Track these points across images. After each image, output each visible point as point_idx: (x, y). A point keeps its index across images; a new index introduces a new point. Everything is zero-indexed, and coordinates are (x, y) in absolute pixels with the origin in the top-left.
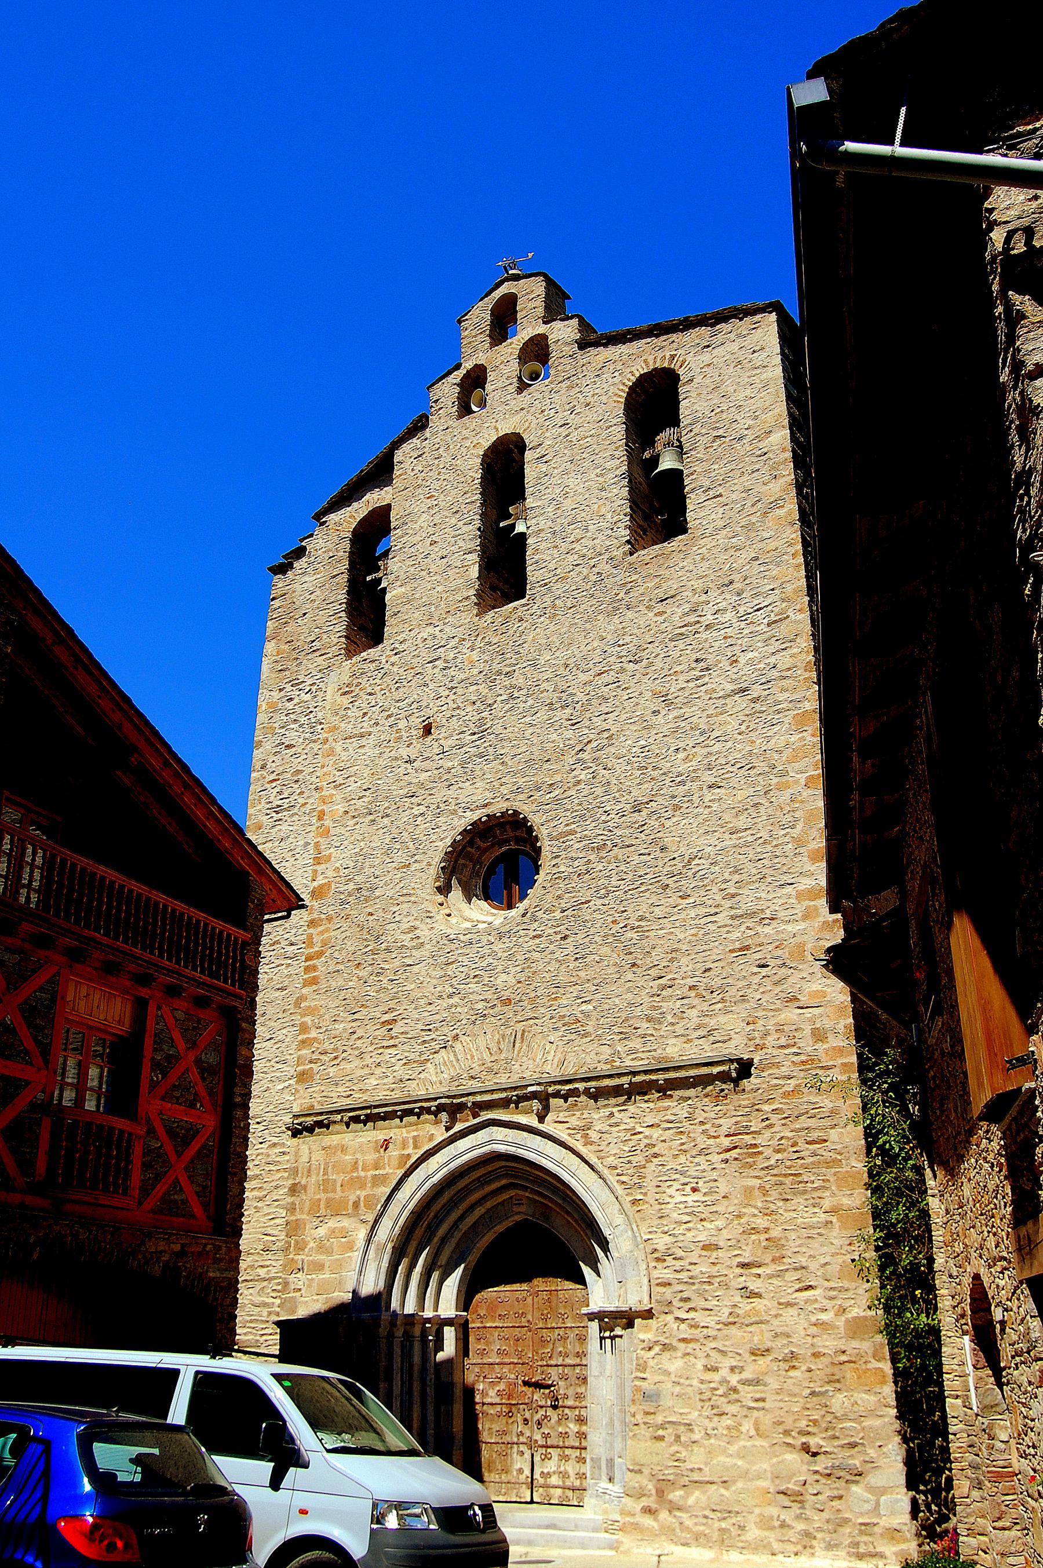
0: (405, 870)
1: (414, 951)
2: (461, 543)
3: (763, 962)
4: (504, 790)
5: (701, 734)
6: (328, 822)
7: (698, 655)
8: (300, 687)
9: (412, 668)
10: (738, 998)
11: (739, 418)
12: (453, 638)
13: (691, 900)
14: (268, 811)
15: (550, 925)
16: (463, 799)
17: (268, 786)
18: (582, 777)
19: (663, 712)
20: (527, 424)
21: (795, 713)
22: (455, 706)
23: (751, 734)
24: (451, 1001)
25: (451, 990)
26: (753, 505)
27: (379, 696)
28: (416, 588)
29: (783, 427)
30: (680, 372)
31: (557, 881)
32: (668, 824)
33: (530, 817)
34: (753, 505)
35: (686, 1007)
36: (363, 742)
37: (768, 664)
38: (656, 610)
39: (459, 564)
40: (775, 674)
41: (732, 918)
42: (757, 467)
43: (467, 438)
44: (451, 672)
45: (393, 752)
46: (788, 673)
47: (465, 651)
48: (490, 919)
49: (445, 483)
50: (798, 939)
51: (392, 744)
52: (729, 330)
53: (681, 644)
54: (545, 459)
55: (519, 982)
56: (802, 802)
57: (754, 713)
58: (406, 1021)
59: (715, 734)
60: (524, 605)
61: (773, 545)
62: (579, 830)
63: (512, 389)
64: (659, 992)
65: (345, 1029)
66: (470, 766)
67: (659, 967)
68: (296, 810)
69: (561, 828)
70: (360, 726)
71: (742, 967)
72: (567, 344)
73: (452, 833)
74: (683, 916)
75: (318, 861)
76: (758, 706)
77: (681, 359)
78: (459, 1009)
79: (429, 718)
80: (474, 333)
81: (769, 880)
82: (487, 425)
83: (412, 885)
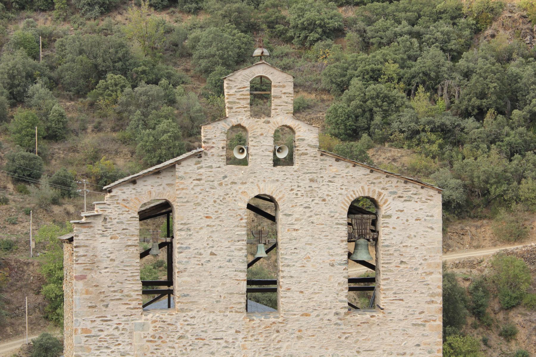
8: (109, 323)
20: (280, 196)
29: (440, 273)
43: (235, 183)
52: (415, 192)
61: (428, 340)
77: (385, 198)
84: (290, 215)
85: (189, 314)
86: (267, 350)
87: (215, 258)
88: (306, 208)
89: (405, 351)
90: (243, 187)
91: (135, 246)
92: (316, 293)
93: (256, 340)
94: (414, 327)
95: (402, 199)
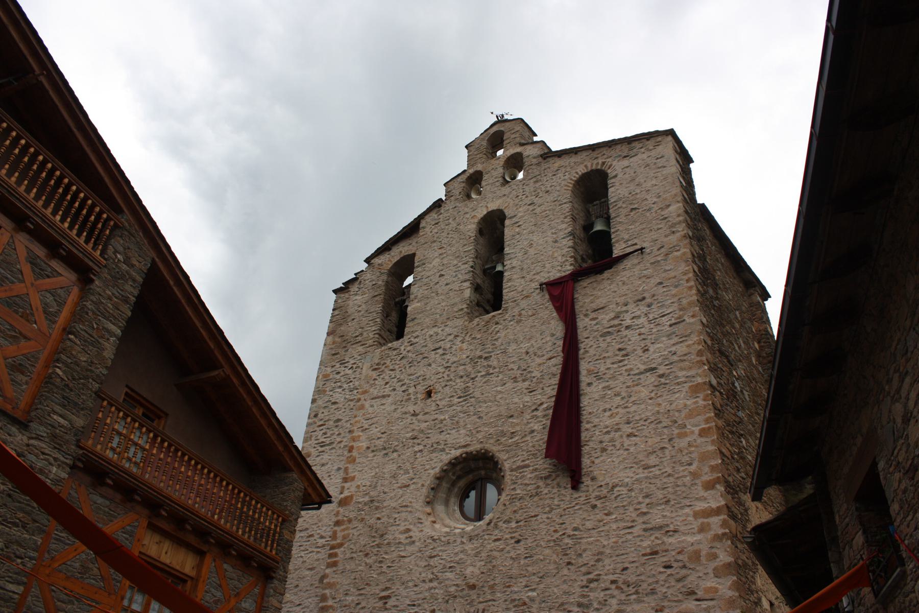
0: (405, 489)
1: (407, 548)
2: (460, 276)
3: (669, 563)
4: (480, 436)
5: (623, 398)
6: (355, 453)
7: (620, 346)
8: (346, 365)
9: (421, 354)
10: (648, 590)
11: (647, 197)
12: (450, 335)
13: (614, 517)
14: (316, 446)
15: (507, 532)
16: (450, 441)
17: (318, 429)
18: (536, 428)
19: (595, 384)
20: (506, 205)
21: (690, 384)
22: (449, 378)
23: (659, 399)
24: (432, 585)
25: (432, 576)
26: (658, 250)
27: (398, 372)
28: (427, 303)
30: (609, 171)
31: (514, 500)
32: (597, 461)
33: (497, 454)
34: (658, 250)
35: (608, 596)
36: (384, 401)
37: (670, 352)
38: (591, 317)
39: (457, 289)
40: (675, 358)
41: (645, 530)
42: (660, 226)
44: (447, 357)
45: (404, 409)
46: (685, 358)
47: (458, 343)
48: (463, 526)
49: (452, 239)
50: (696, 547)
51: (403, 403)
53: (608, 339)
54: (518, 225)
55: (483, 573)
56: (696, 446)
57: (661, 385)
58: (398, 598)
59: (633, 399)
60: (500, 314)
61: (672, 274)
62: (531, 464)
63: (498, 184)
64: (588, 584)
65: (353, 601)
66: (456, 419)
67: (589, 565)
68: (334, 446)
69: (519, 463)
70: (383, 390)
71: (652, 567)
72: (534, 158)
73: (440, 464)
74: (606, 528)
75: (345, 480)
76: (663, 380)
77: (609, 164)
78: (437, 591)
79: (430, 386)
80: (476, 153)
81: (672, 503)
82: (481, 205)
83: (410, 499)
84: (515, 216)
85: (414, 335)
86: (483, 345)
87: (442, 279)
88: (529, 205)
89: (643, 295)
91: (380, 295)
92: (538, 273)
93: (473, 338)
94: (653, 266)
95: (628, 158)
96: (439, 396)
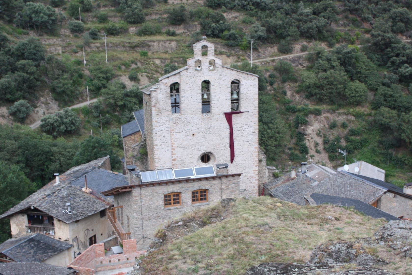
6: (174, 147)
44: (198, 125)
90: (200, 78)
96: (197, 136)
